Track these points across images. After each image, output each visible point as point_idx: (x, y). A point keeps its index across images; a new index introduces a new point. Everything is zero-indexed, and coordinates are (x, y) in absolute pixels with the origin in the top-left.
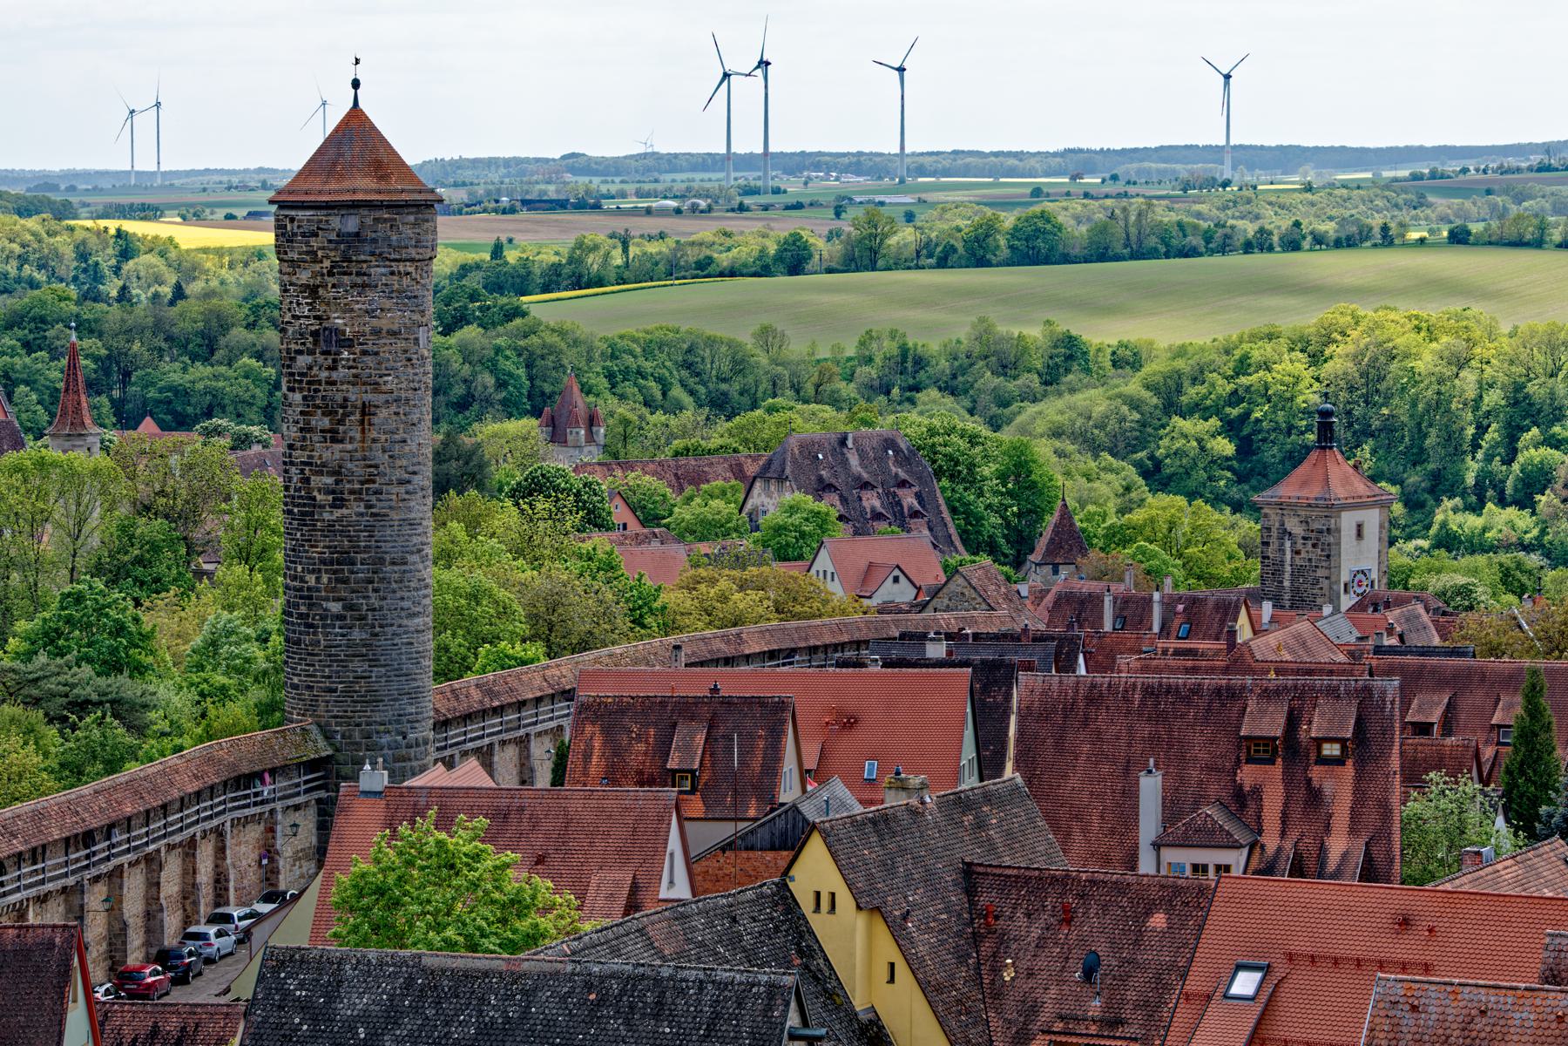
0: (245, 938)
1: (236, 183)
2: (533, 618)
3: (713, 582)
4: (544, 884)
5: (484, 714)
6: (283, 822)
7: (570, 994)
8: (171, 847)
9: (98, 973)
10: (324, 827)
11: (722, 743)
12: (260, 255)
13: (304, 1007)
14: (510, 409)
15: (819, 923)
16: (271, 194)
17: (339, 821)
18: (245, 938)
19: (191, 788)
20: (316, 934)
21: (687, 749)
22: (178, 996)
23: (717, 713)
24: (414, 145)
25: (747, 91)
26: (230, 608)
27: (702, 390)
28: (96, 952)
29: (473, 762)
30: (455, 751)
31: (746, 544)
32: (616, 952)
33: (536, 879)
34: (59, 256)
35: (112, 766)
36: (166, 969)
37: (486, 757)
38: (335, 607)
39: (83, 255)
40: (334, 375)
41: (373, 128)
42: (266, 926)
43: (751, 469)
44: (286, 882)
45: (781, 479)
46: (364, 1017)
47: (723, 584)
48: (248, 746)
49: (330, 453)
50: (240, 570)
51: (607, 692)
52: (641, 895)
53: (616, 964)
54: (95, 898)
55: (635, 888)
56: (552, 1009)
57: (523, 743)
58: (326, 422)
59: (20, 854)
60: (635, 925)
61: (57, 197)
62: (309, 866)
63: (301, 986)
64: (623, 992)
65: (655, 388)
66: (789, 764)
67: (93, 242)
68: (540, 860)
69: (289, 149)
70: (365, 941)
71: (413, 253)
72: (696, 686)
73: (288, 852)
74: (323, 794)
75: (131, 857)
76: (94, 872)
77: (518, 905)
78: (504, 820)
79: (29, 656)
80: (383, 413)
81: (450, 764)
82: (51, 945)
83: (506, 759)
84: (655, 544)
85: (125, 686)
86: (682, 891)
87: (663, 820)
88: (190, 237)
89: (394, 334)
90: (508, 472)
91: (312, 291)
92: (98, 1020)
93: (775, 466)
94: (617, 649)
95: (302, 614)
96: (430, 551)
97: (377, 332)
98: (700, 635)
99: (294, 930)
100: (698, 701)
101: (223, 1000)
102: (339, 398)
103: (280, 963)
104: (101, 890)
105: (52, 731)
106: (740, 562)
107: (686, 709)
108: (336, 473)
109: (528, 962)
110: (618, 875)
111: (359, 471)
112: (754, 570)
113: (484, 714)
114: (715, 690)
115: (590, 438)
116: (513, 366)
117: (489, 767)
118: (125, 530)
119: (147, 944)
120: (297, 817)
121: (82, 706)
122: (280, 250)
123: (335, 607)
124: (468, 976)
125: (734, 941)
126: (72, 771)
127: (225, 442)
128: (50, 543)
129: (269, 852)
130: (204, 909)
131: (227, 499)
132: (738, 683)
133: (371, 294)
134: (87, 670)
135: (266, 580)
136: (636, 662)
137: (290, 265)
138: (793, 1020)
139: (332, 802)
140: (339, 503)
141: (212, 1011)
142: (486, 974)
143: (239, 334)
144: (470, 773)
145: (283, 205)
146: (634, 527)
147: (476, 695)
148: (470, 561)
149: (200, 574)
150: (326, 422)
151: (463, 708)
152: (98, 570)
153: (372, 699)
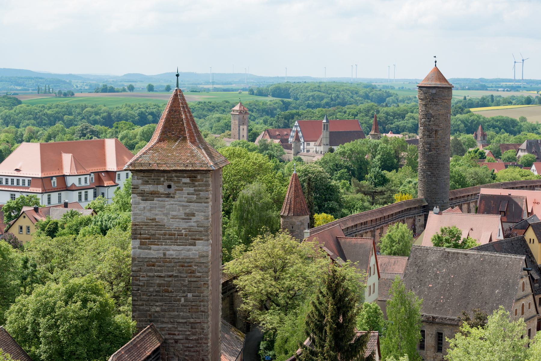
6: (417, 218)
15: (531, 246)
25: (519, 66)
46: (433, 261)
57: (469, 204)
73: (418, 225)
74: (426, 213)
75: (385, 225)
76: (377, 228)
80: (440, 132)
102: (431, 128)
108: (430, 144)
111: (435, 144)
120: (420, 218)
139: (428, 215)
140: (430, 151)
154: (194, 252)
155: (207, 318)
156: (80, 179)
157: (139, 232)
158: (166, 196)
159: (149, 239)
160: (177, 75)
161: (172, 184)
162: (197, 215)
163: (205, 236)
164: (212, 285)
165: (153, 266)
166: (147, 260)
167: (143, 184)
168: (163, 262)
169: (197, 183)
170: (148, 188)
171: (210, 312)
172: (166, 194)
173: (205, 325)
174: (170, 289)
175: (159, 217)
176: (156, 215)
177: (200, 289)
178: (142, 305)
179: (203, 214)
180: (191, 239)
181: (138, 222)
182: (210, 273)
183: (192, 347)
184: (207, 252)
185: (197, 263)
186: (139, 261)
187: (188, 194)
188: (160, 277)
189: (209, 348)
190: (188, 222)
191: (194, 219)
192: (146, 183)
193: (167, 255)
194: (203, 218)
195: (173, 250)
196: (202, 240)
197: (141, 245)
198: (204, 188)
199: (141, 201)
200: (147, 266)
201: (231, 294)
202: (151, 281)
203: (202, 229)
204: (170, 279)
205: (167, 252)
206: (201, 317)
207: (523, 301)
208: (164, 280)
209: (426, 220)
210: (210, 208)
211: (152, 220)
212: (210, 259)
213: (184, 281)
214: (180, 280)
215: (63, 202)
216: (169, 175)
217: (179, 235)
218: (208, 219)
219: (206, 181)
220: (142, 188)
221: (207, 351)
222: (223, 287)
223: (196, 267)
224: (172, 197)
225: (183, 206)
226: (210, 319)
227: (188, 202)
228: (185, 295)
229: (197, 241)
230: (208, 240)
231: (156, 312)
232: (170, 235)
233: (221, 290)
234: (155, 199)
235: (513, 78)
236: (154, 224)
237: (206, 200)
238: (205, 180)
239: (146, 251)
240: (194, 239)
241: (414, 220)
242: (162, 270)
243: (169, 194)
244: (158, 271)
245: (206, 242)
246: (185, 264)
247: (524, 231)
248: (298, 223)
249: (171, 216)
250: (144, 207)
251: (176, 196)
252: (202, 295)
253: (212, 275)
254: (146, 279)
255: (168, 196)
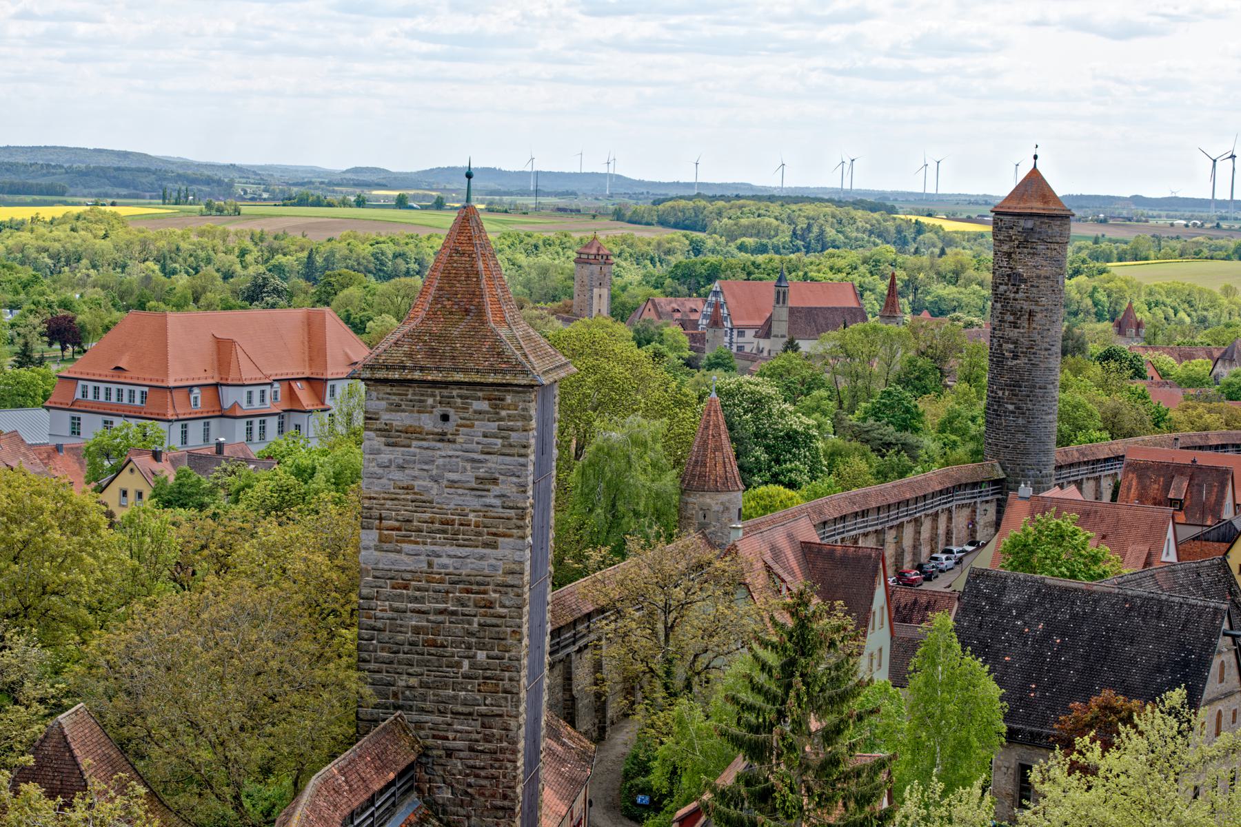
0: (959, 562)
1: (973, 201)
2: (1105, 420)
3: (1195, 408)
4: (1105, 548)
5: (1079, 464)
6: (980, 508)
7: (1116, 604)
8: (927, 516)
9: (890, 572)
10: (1000, 512)
11: (1195, 489)
12: (982, 235)
13: (987, 598)
14: (1100, 317)
16: (992, 208)
17: (1007, 510)
18: (959, 562)
19: (938, 488)
20: (993, 563)
21: (1179, 489)
22: (926, 586)
23: (1194, 472)
24: (1062, 185)
26: (959, 404)
27: (1194, 314)
28: (889, 562)
29: (1073, 487)
30: (1065, 481)
31: (1212, 390)
32: (1139, 585)
33: (1102, 546)
34: (888, 231)
35: (902, 475)
36: (922, 573)
37: (1079, 484)
38: (1011, 407)
39: (899, 231)
40: (1017, 296)
41: (1042, 178)
42: (970, 557)
43: (1217, 354)
44: (980, 537)
45: (1231, 360)
47: (1200, 410)
48: (966, 471)
49: (1014, 333)
50: (965, 385)
51: (1141, 458)
52: (1152, 558)
53: (1139, 591)
54: (890, 537)
55: (1149, 555)
56: (1107, 610)
57: (1098, 479)
58: (1012, 318)
59: (857, 513)
60: (1149, 573)
61: (889, 203)
62: (992, 531)
63: (987, 587)
64: (1142, 605)
65: (1171, 312)
66: (1229, 500)
67: (904, 225)
68: (1104, 537)
69: (1002, 186)
70: (1015, 569)
71: (1058, 239)
72: (1185, 458)
74: (1000, 496)
77: (1095, 559)
78: (1086, 516)
79: (864, 420)
80: (1039, 316)
81: (1062, 487)
82: (870, 557)
83: (1089, 486)
84: (1167, 388)
85: (908, 437)
86: (1173, 558)
87: (1165, 523)
88: (950, 226)
89: (1047, 278)
90: (1095, 348)
91: (1009, 255)
92: (889, 595)
93: (1229, 353)
94: (1146, 438)
95: (994, 411)
96: (1058, 384)
97: (1039, 277)
98: (1187, 433)
99: (984, 560)
100: (1185, 466)
101: (948, 590)
103: (977, 576)
104: (893, 533)
105: (873, 455)
106: (1208, 399)
107: (1180, 469)
108: (1015, 343)
109: (1097, 586)
110: (1141, 548)
112: (1216, 404)
113: (1079, 464)
114: (1194, 461)
115: (1137, 334)
116: (1101, 296)
117: (1080, 489)
118: (911, 362)
119: (913, 560)
120: (987, 506)
121: (889, 445)
122: (994, 235)
123: (1011, 407)
124: (1067, 590)
125: (1198, 585)
126: (882, 475)
127: (961, 324)
128: (876, 367)
129: (973, 521)
130: (941, 546)
131: (961, 352)
132: (1206, 459)
133: (1037, 258)
134: (891, 428)
135: (977, 392)
136: (1155, 445)
137: (999, 242)
138: (1226, 626)
139: (1005, 500)
140: (1016, 357)
141: (943, 595)
142: (1076, 590)
143: (970, 272)
144: (1071, 492)
145: (997, 213)
146: (1157, 378)
147: (1076, 454)
148: (1078, 390)
149: (946, 386)
150: (1012, 318)
151: (1069, 460)
152: (899, 382)
153: (1026, 453)
154: (493, 562)
155: (517, 707)
156: (250, 393)
157: (376, 513)
158: (438, 437)
159: (399, 529)
160: (469, 176)
161: (451, 412)
162: (503, 482)
163: (519, 527)
164: (530, 636)
165: (406, 587)
166: (393, 574)
167: (388, 410)
168: (428, 582)
169: (503, 413)
170: (401, 420)
171: (523, 694)
172: (437, 434)
173: (513, 723)
174: (440, 639)
175: (421, 483)
176: (415, 478)
177: (503, 642)
178: (379, 672)
179: (514, 479)
180: (488, 534)
181: (376, 492)
182: (526, 609)
183: (483, 768)
184: (521, 563)
185: (498, 585)
186: (375, 577)
187: (485, 436)
188: (419, 612)
189: (519, 771)
190: (482, 496)
191: (496, 490)
192: (397, 408)
193: (435, 566)
194: (514, 490)
195: (449, 556)
196: (510, 536)
197: (380, 541)
198: (519, 424)
199: (383, 448)
200: (393, 588)
201: (568, 655)
202: (399, 622)
203: (512, 513)
204: (440, 618)
205: (436, 560)
206: (503, 703)
207: (1219, 706)
208: (428, 621)
209: (1000, 512)
210: (531, 468)
211: (407, 488)
212: (527, 578)
213: (470, 623)
214: (463, 622)
215: (213, 441)
216: (445, 392)
217: (462, 525)
218: (525, 492)
219: (523, 409)
220: (385, 417)
221: (515, 777)
222: (552, 639)
223: (497, 595)
224: (449, 441)
225: (473, 460)
226: (522, 709)
227: (483, 453)
228: (471, 654)
229: (500, 539)
230: (523, 538)
231: (408, 687)
232: (442, 523)
233: (547, 648)
234: (414, 443)
235: (1228, 198)
236: (409, 497)
237: (522, 451)
238: (521, 405)
239: (392, 555)
240: (495, 534)
241: (974, 511)
242: (423, 598)
243: (444, 434)
244: (416, 600)
245: (520, 541)
246: (473, 585)
247: (1228, 545)
248: (715, 508)
249: (445, 482)
250: (390, 461)
251: (460, 439)
252: (507, 655)
253: (530, 613)
254: (390, 614)
255: (442, 437)
